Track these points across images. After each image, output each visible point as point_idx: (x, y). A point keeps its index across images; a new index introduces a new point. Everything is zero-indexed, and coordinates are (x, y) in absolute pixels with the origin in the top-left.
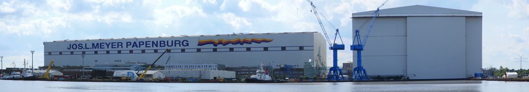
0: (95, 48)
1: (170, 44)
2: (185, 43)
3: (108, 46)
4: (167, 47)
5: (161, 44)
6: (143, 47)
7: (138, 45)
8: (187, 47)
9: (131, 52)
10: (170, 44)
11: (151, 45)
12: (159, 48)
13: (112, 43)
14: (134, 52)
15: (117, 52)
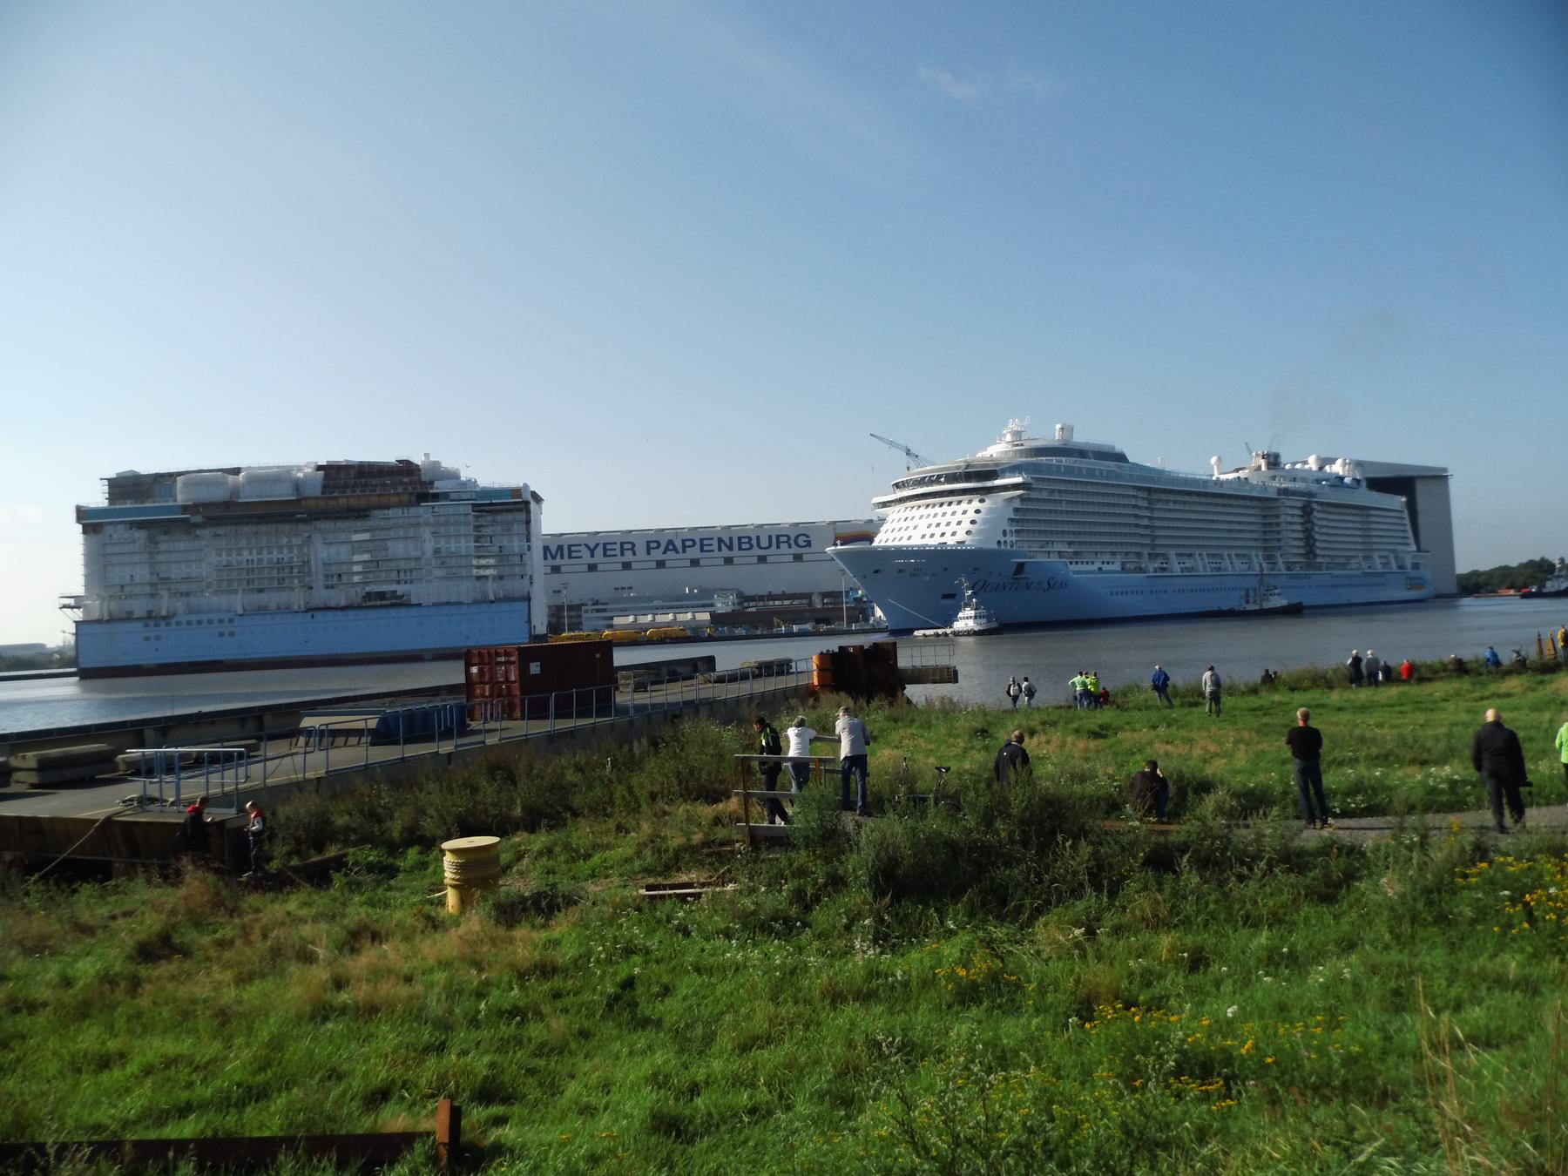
0: (554, 558)
1: (764, 543)
2: (801, 541)
3: (592, 552)
4: (757, 551)
5: (740, 543)
6: (694, 553)
7: (680, 548)
8: (807, 549)
9: (661, 564)
10: (764, 543)
11: (715, 547)
12: (736, 552)
13: (605, 545)
14: (668, 564)
15: (620, 566)
